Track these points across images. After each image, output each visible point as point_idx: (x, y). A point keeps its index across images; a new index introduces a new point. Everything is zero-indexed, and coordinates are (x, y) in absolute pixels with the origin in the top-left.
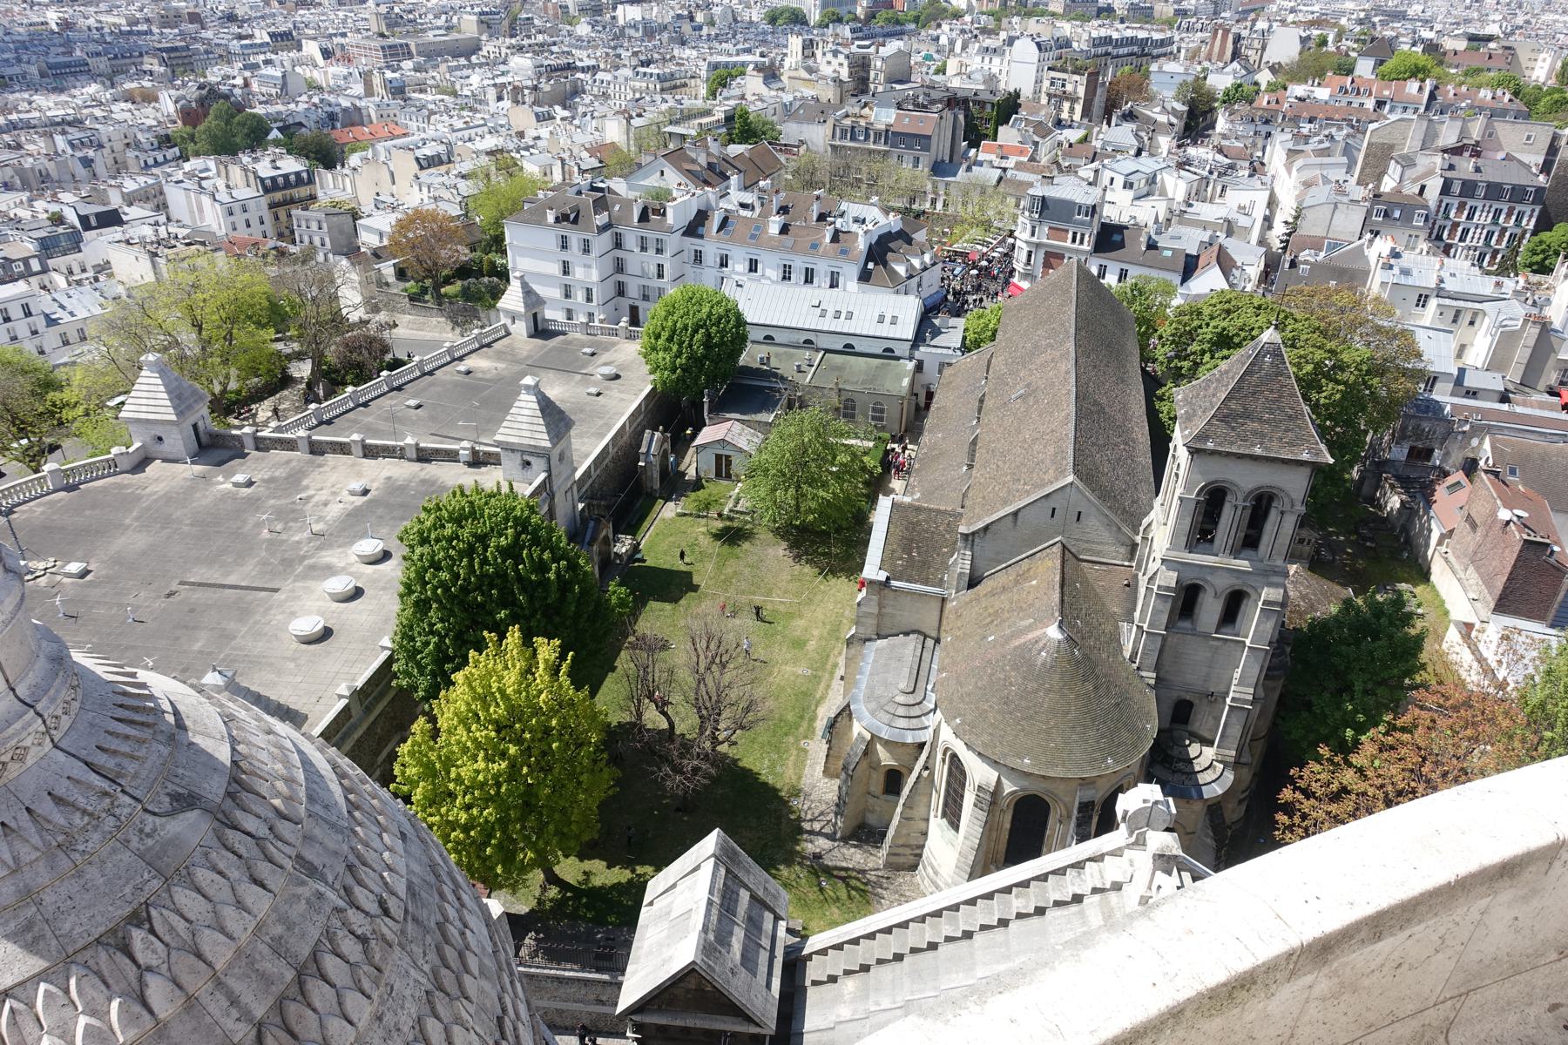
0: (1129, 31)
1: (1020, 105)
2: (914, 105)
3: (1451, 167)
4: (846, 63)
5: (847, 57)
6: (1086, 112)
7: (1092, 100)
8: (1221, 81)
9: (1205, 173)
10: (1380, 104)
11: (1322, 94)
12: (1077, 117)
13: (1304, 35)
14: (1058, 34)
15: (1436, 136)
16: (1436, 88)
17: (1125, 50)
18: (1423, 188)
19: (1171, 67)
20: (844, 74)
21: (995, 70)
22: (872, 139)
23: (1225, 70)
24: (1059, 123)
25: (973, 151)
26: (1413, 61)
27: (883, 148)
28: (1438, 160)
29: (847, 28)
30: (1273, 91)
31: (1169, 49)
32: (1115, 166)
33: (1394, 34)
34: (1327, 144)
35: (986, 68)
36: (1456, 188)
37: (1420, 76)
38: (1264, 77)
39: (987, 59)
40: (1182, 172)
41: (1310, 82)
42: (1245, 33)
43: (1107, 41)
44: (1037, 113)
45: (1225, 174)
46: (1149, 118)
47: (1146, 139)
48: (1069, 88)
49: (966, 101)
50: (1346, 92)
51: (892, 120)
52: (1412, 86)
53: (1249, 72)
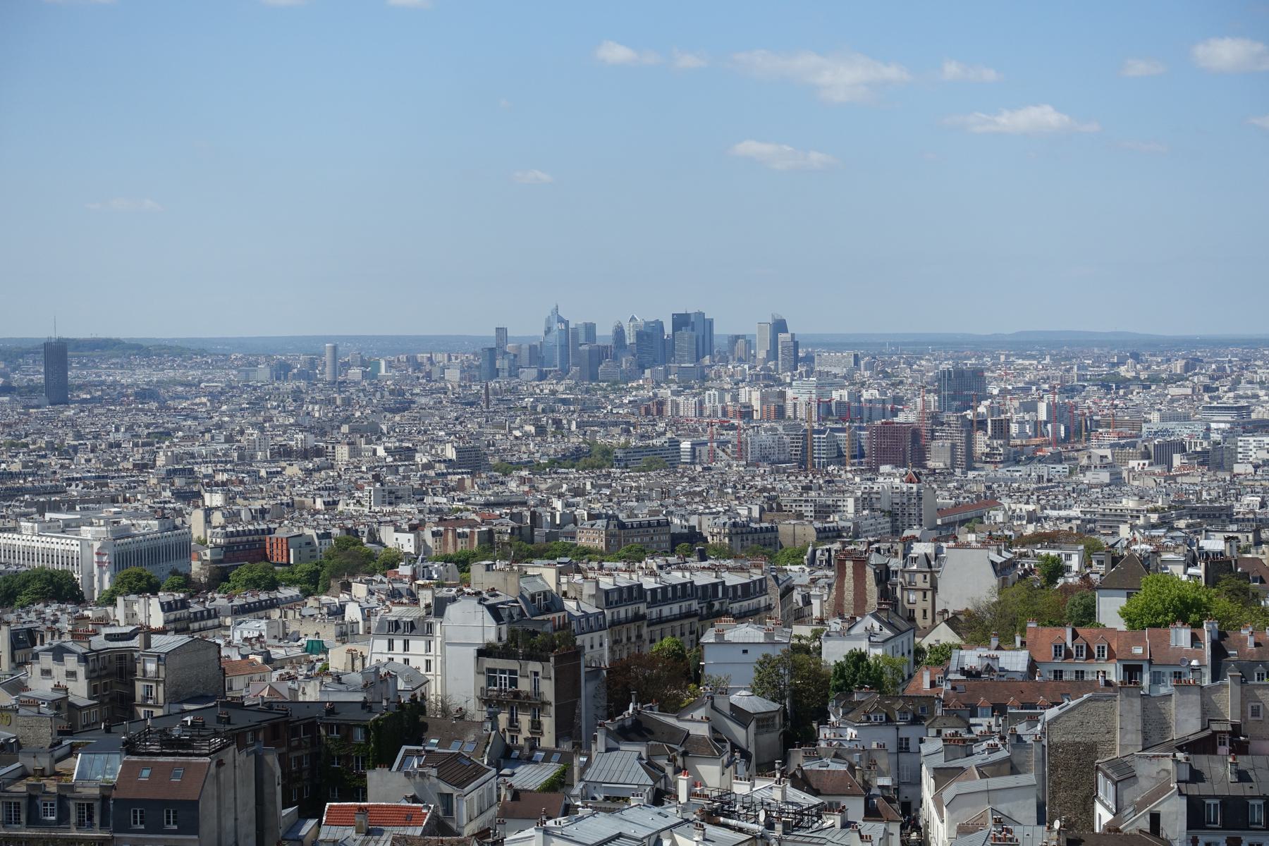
0: (679, 574)
1: (425, 727)
2: (163, 744)
3: (1196, 776)
4: (81, 671)
5: (83, 658)
6: (566, 728)
7: (574, 705)
8: (834, 653)
9: (758, 828)
10: (1132, 671)
11: (1015, 661)
12: (548, 740)
13: (999, 560)
14: (530, 588)
15: (1164, 726)
16: (1222, 635)
17: (676, 609)
18: (1155, 819)
19: (747, 632)
20: (79, 691)
21: (417, 662)
22: (73, 819)
23: (853, 632)
24: (507, 756)
25: (311, 823)
26: (1175, 592)
27: (98, 834)
28: (1167, 766)
29: (155, 602)
30: (939, 662)
31: (763, 601)
32: (572, 830)
33: (1150, 548)
34: (1003, 753)
35: (399, 660)
36: (1214, 814)
37: (1193, 617)
38: (944, 635)
39: (399, 644)
40: (711, 830)
41: (994, 642)
42: (895, 563)
43: (636, 593)
44: (460, 738)
45: (798, 826)
46: (674, 731)
47: (669, 770)
48: (524, 685)
49: (311, 726)
50: (1068, 654)
51: (113, 778)
52: (1181, 636)
53: (898, 632)
